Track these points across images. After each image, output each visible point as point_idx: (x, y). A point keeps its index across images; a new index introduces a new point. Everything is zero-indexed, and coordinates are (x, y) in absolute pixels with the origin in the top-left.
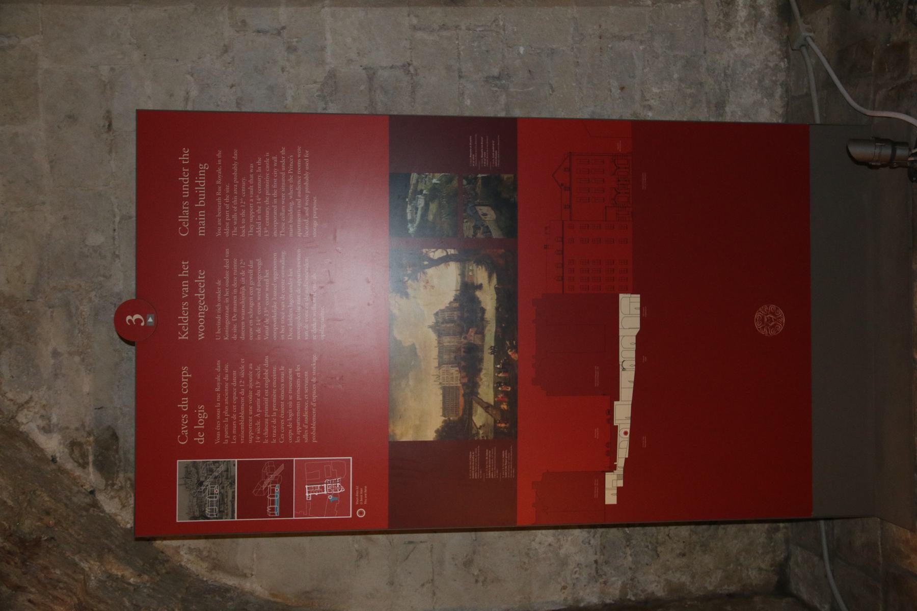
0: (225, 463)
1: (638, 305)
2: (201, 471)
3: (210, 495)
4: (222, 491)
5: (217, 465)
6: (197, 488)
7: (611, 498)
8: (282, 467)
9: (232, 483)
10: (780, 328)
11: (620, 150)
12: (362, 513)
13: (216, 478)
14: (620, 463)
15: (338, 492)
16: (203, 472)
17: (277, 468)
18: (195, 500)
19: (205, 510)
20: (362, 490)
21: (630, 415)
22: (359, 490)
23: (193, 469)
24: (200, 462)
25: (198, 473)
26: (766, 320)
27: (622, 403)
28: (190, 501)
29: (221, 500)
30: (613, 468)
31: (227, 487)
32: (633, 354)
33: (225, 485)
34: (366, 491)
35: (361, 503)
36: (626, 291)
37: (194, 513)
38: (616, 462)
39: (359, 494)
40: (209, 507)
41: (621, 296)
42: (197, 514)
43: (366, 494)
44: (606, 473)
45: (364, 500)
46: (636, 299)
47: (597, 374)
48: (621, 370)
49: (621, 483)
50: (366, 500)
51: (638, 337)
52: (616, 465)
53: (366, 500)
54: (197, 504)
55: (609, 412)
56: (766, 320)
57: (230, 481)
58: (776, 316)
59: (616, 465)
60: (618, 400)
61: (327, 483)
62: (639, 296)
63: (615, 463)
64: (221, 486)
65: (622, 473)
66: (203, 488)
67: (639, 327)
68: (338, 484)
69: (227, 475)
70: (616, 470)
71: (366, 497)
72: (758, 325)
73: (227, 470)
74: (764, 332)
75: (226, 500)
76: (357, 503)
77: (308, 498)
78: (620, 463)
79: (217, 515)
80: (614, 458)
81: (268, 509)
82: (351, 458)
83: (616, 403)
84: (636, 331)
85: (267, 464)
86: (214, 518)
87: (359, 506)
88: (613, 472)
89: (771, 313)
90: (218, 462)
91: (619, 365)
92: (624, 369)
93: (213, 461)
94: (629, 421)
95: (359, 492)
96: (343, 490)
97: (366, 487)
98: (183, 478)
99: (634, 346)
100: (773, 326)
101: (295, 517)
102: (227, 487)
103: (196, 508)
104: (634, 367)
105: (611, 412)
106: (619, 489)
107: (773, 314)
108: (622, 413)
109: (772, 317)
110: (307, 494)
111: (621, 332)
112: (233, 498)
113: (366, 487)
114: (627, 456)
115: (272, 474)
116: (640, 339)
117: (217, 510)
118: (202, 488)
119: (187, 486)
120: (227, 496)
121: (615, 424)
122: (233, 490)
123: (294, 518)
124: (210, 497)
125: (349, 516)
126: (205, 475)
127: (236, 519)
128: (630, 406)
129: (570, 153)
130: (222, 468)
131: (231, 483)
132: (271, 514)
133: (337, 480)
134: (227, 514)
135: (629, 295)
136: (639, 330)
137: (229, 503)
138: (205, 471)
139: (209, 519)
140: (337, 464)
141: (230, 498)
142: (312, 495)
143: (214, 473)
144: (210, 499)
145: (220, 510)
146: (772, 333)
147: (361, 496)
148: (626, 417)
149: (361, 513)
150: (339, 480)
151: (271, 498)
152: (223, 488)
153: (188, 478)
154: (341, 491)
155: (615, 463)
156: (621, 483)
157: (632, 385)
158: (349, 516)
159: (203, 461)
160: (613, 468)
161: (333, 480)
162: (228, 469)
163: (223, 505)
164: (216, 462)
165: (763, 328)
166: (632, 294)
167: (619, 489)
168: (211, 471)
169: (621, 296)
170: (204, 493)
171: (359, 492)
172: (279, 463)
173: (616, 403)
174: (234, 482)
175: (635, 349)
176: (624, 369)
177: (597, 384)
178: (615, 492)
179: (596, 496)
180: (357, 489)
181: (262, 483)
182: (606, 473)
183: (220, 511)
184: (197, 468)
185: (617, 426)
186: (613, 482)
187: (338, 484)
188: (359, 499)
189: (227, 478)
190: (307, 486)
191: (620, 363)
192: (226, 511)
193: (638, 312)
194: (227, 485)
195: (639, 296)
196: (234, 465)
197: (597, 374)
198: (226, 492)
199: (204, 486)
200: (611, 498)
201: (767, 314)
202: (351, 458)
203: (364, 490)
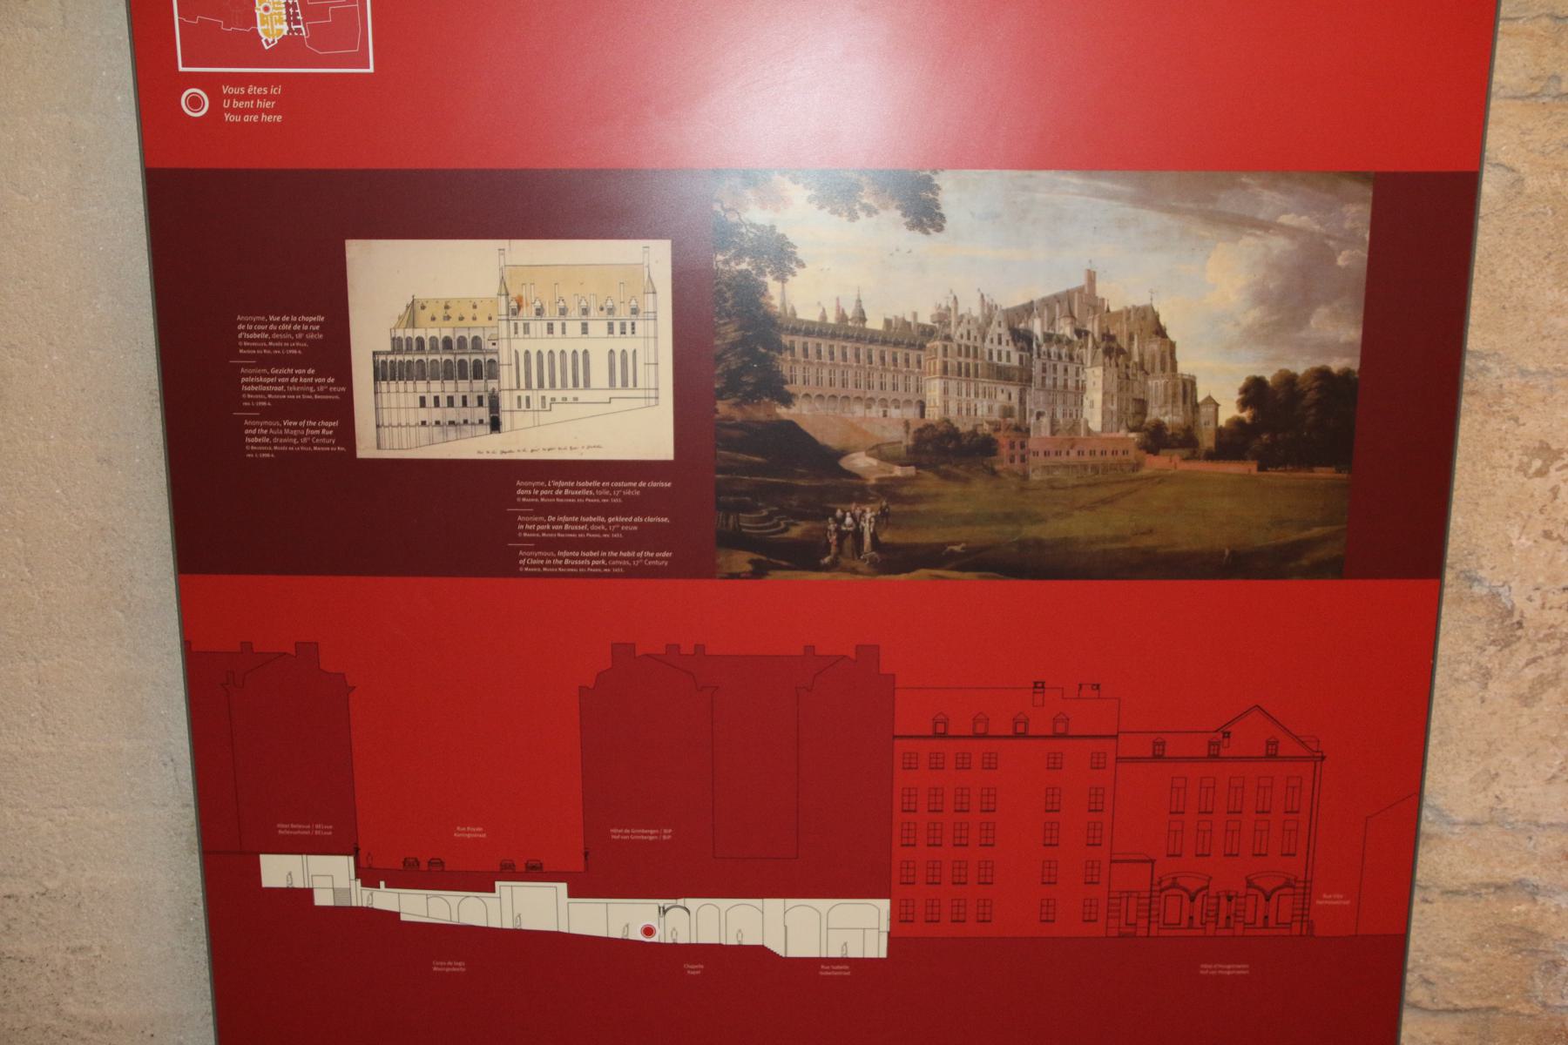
1: (855, 953)
7: (277, 871)
11: (1319, 902)
12: (194, 104)
14: (384, 899)
20: (268, 104)
22: (269, 97)
27: (562, 907)
30: (367, 876)
32: (708, 937)
34: (269, 118)
36: (896, 917)
38: (387, 886)
39: (254, 97)
41: (884, 905)
44: (351, 859)
46: (877, 948)
47: (650, 835)
48: (662, 902)
49: (323, 899)
50: (237, 119)
51: (761, 952)
53: (237, 119)
55: (533, 867)
60: (572, 894)
62: (883, 954)
63: (382, 884)
65: (354, 904)
67: (790, 955)
70: (364, 885)
71: (247, 118)
78: (384, 899)
82: (371, 70)
83: (563, 887)
87: (216, 98)
88: (357, 876)
91: (676, 897)
92: (665, 912)
94: (508, 925)
95: (262, 97)
97: (279, 118)
99: (732, 941)
104: (669, 941)
105: (534, 872)
106: (308, 893)
111: (774, 905)
114: (404, 918)
121: (498, 884)
125: (183, 66)
128: (554, 929)
129: (1323, 758)
133: (297, 22)
135: (885, 926)
136: (780, 951)
147: (250, 104)
148: (519, 916)
149: (195, 103)
150: (299, 31)
154: (264, 37)
155: (382, 884)
161: (298, 11)
166: (889, 934)
167: (308, 893)
169: (884, 905)
171: (262, 97)
173: (563, 887)
175: (724, 942)
178: (298, 883)
179: (283, 829)
180: (273, 91)
182: (351, 859)
185: (493, 890)
188: (240, 98)
191: (681, 902)
193: (835, 953)
195: (883, 954)
197: (650, 835)
200: (277, 871)
202: (371, 70)
203: (268, 112)
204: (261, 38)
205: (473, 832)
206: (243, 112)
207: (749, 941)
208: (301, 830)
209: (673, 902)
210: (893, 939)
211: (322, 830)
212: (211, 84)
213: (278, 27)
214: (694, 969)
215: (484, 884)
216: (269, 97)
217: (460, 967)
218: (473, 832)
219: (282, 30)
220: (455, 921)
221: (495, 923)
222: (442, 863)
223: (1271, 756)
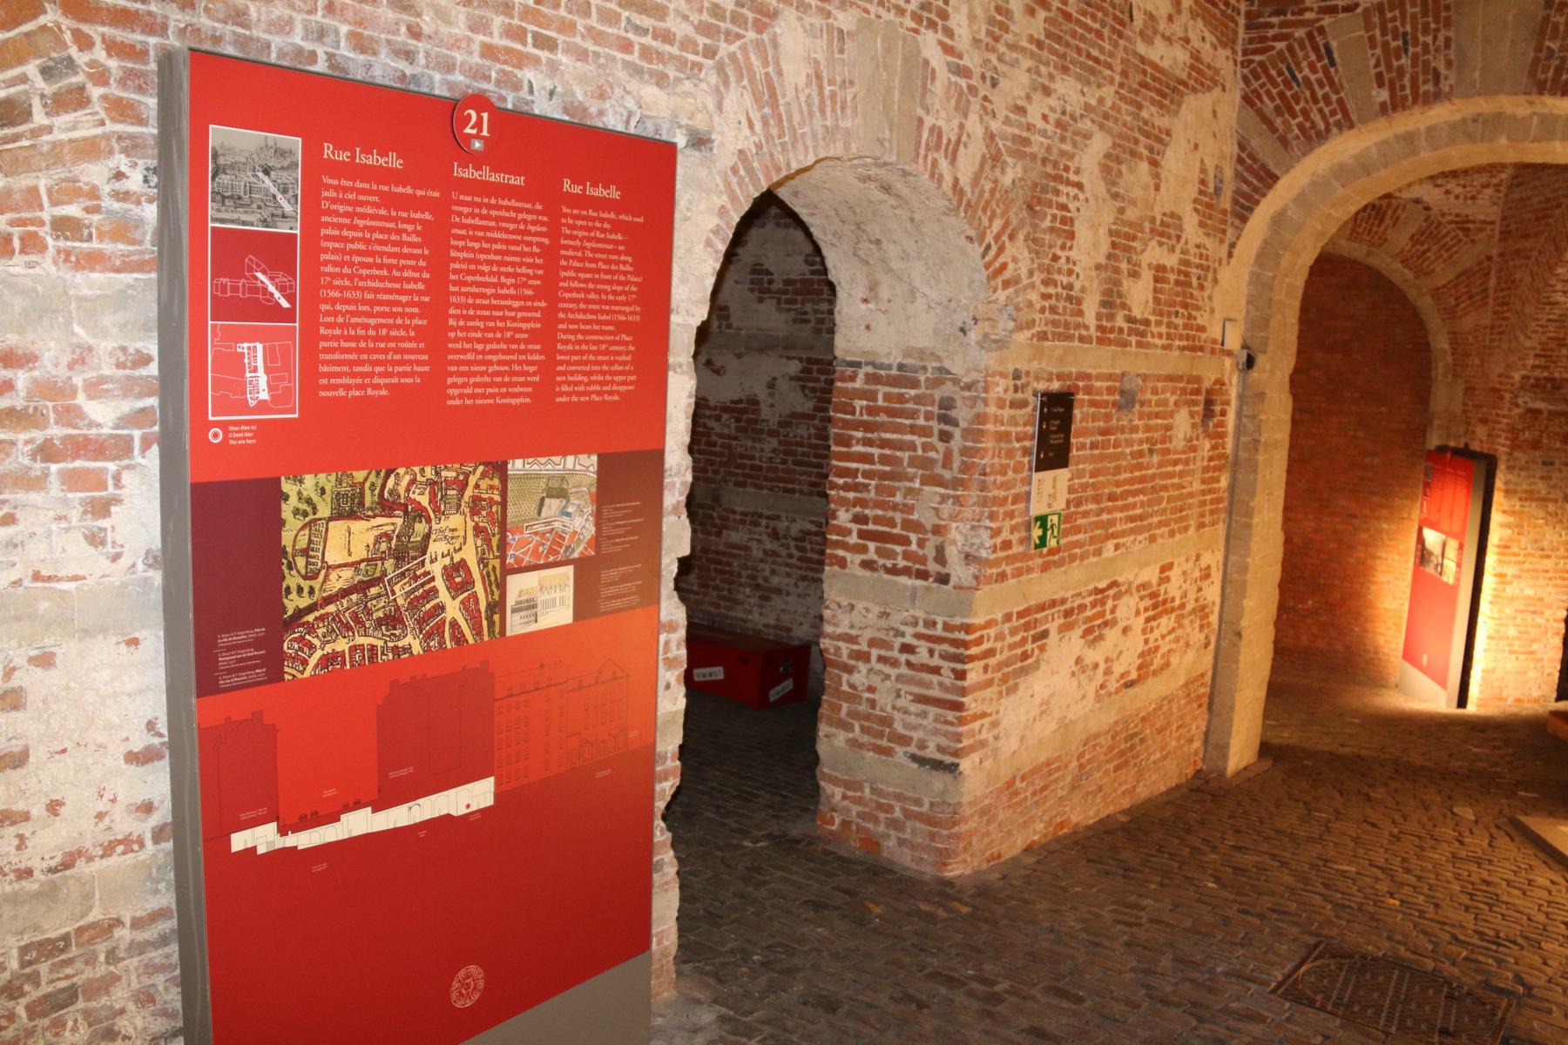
1: (482, 806)
2: (284, 174)
7: (240, 841)
8: (285, 304)
9: (264, 222)
12: (215, 436)
13: (274, 197)
16: (284, 177)
18: (243, 160)
21: (355, 834)
23: (286, 164)
25: (282, 168)
30: (283, 831)
32: (428, 816)
36: (497, 785)
42: (221, 161)
47: (403, 772)
49: (261, 850)
51: (448, 816)
66: (260, 174)
73: (284, 216)
80: (298, 827)
81: (224, 280)
83: (369, 809)
84: (455, 814)
87: (226, 432)
96: (252, 403)
103: (230, 160)
105: (358, 805)
106: (255, 848)
108: (359, 823)
112: (244, 223)
116: (444, 822)
127: (210, 225)
130: (288, 208)
137: (235, 216)
139: (213, 178)
140: (288, 392)
141: (244, 217)
146: (454, 995)
149: (216, 436)
156: (261, 850)
160: (283, 831)
167: (255, 848)
168: (284, 191)
169: (492, 779)
173: (369, 809)
177: (392, 775)
178: (250, 845)
179: (243, 817)
181: (264, 272)
183: (224, 197)
184: (289, 167)
186: (262, 838)
197: (403, 772)
200: (240, 841)
207: (444, 812)
208: (251, 814)
210: (497, 796)
211: (262, 811)
212: (224, 426)
214: (422, 834)
217: (324, 866)
220: (323, 842)
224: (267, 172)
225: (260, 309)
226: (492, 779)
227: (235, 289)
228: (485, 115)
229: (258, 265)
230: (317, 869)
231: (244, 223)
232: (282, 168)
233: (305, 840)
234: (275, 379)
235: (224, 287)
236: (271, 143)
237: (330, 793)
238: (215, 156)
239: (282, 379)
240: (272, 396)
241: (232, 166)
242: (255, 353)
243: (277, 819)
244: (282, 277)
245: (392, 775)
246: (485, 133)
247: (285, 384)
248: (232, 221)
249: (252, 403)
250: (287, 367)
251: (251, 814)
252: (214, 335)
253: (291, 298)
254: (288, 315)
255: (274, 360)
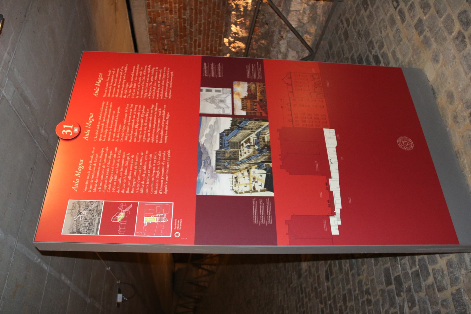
0: (97, 203)
1: (334, 134)
2: (82, 206)
3: (85, 220)
4: (93, 218)
5: (92, 203)
6: (78, 216)
7: (335, 231)
8: (131, 206)
9: (99, 214)
10: (412, 147)
12: (178, 235)
13: (90, 210)
15: (164, 222)
16: (83, 206)
17: (127, 208)
18: (75, 222)
19: (80, 229)
20: (178, 221)
21: (339, 186)
22: (177, 221)
23: (78, 206)
24: (82, 201)
25: (79, 207)
26: (403, 143)
28: (72, 223)
29: (91, 223)
30: (333, 214)
31: (95, 216)
32: (335, 156)
33: (95, 215)
34: (181, 222)
35: (178, 229)
36: (327, 127)
37: (73, 229)
38: (335, 210)
39: (177, 224)
40: (83, 227)
42: (75, 230)
43: (181, 224)
44: (330, 217)
45: (179, 228)
46: (333, 131)
47: (317, 165)
49: (340, 223)
51: (337, 148)
52: (335, 212)
54: (76, 225)
56: (403, 143)
57: (98, 212)
58: (408, 141)
59: (335, 212)
60: (331, 178)
61: (157, 216)
63: (334, 211)
64: (92, 215)
66: (81, 215)
68: (164, 217)
69: (97, 209)
71: (181, 225)
72: (400, 145)
73: (97, 207)
74: (404, 148)
75: (94, 223)
76: (175, 229)
77: (145, 225)
79: (87, 231)
80: (333, 209)
81: (119, 230)
83: (330, 179)
84: (336, 145)
85: (122, 205)
86: (85, 234)
87: (177, 231)
88: (334, 216)
89: (405, 140)
90: (93, 202)
93: (90, 201)
94: (339, 189)
95: (177, 222)
96: (167, 220)
97: (181, 220)
98: (70, 209)
100: (408, 146)
101: (136, 235)
102: (95, 216)
103: (75, 227)
105: (328, 184)
106: (339, 226)
107: (407, 140)
109: (406, 142)
110: (144, 222)
111: (327, 146)
112: (99, 222)
113: (181, 220)
114: (341, 208)
115: (124, 210)
116: (338, 149)
117: (88, 229)
118: (81, 215)
119: (72, 214)
120: (95, 221)
121: (331, 191)
122: (99, 218)
123: (135, 236)
124: (85, 221)
125: (170, 236)
126: (84, 208)
127: (98, 235)
130: (95, 205)
131: (98, 214)
132: (121, 233)
134: (93, 231)
137: (96, 225)
138: (84, 206)
140: (164, 206)
142: (147, 223)
143: (90, 208)
144: (84, 222)
145: (90, 228)
146: (408, 149)
147: (178, 225)
149: (177, 235)
150: (165, 215)
151: (121, 224)
152: (93, 216)
153: (73, 210)
154: (166, 221)
155: (334, 211)
157: (338, 171)
158: (170, 236)
159: (84, 201)
160: (333, 214)
162: (98, 206)
163: (91, 226)
164: (92, 202)
165: (403, 146)
167: (339, 226)
168: (88, 206)
169: (324, 129)
170: (81, 218)
171: (177, 222)
172: (128, 204)
173: (330, 179)
174: (101, 213)
176: (332, 163)
177: (317, 170)
178: (337, 227)
179: (326, 230)
182: (330, 217)
183: (89, 230)
187: (164, 217)
189: (97, 211)
190: (145, 218)
191: (329, 160)
192: (93, 230)
193: (335, 137)
194: (96, 215)
195: (334, 130)
196: (102, 204)
197: (317, 165)
198: (95, 219)
199: (82, 215)
200: (335, 231)
201: (404, 141)
203: (180, 221)
204: (166, 222)
205: (321, 194)
206: (179, 226)
207: (335, 150)
208: (325, 226)
209: (329, 162)
210: (331, 128)
211: (325, 222)
212: (174, 231)
213: (164, 218)
214: (342, 159)
215: (331, 194)
216: (177, 221)
217: (349, 198)
218: (321, 194)
219: (165, 218)
221: (339, 192)
222: (328, 200)
223: (291, 78)
224: (80, 213)
225: (131, 217)
226: (324, 129)
227: (123, 226)
228: (65, 126)
229: (115, 217)
230: (350, 202)
231: (99, 222)
232: (79, 207)
233: (338, 205)
234: (158, 211)
235: (122, 230)
236: (70, 211)
237: (321, 195)
238: (73, 233)
239: (159, 208)
240: (165, 212)
241: (77, 226)
242: (148, 220)
243: (328, 216)
244: (120, 208)
245: (317, 170)
246: (71, 127)
247: (160, 207)
248: (98, 226)
249: (167, 220)
250: (154, 206)
251: (325, 226)
252: (140, 234)
253: (128, 204)
254: (135, 205)
255: (151, 211)
